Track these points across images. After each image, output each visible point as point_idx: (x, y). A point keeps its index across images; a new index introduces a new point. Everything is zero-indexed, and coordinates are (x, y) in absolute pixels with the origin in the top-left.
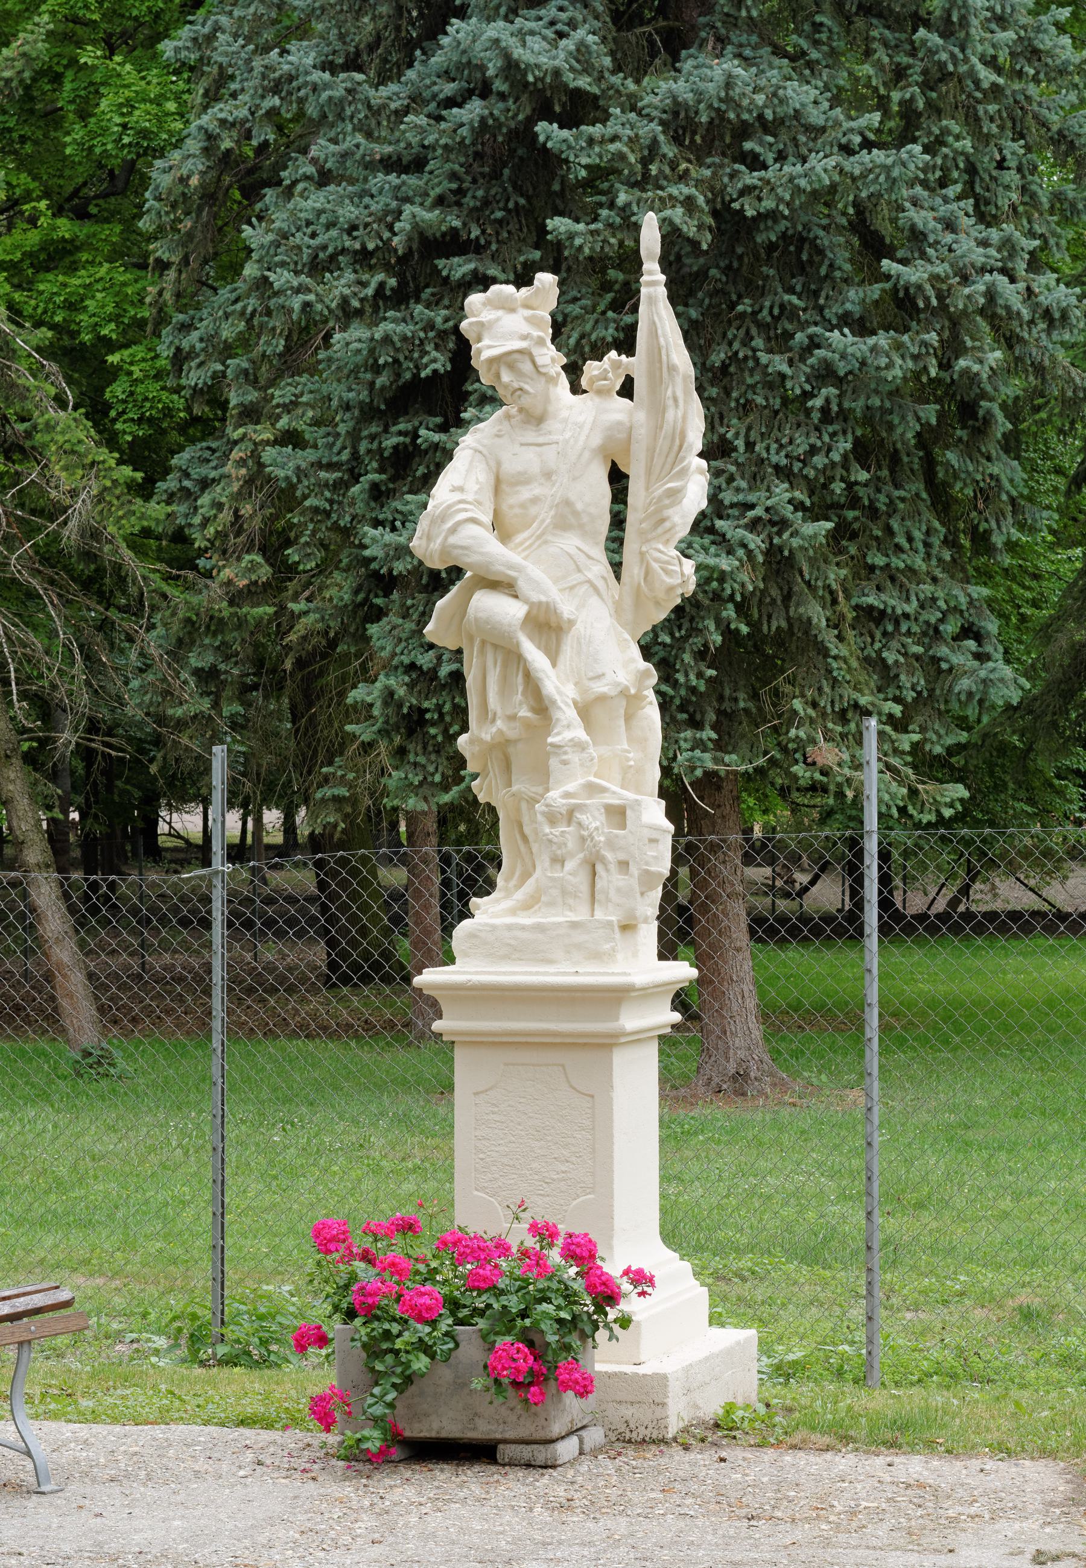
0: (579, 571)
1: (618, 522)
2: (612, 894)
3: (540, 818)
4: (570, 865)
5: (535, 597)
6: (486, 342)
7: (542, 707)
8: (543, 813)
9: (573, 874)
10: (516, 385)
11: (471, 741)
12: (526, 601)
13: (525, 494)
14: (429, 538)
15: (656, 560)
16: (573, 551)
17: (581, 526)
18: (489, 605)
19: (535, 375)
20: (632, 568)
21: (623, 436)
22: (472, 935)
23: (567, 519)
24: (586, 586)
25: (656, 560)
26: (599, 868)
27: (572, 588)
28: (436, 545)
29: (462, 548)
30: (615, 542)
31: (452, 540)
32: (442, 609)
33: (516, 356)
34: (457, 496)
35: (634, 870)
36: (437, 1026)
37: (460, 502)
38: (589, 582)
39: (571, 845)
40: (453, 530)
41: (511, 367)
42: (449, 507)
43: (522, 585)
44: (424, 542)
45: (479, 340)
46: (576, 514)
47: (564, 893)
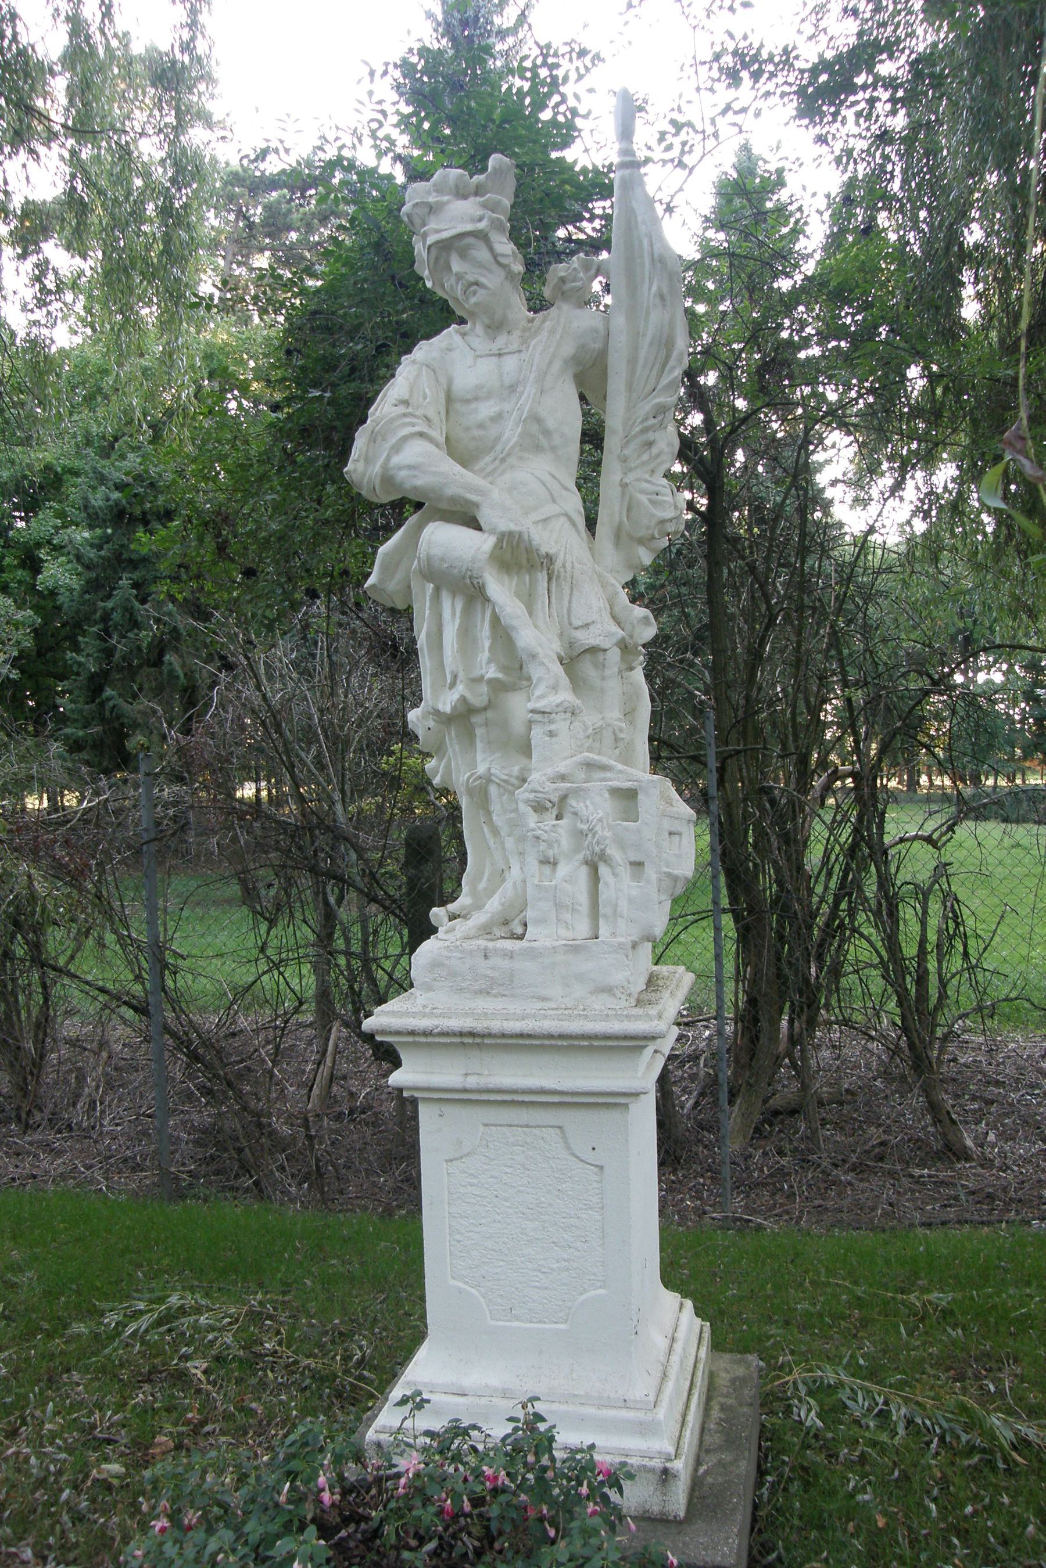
0: (554, 501)
1: (593, 436)
2: (624, 906)
3: (523, 808)
4: (563, 870)
5: (505, 525)
6: (432, 225)
7: (516, 669)
8: (527, 802)
9: (569, 880)
10: (471, 278)
11: (426, 715)
12: (492, 532)
13: (486, 410)
14: (368, 460)
15: (643, 492)
16: (546, 478)
17: (553, 449)
18: (442, 539)
19: (494, 267)
20: (607, 515)
21: (598, 346)
22: (435, 965)
23: (536, 438)
24: (563, 519)
25: (643, 492)
26: (603, 870)
27: (545, 520)
28: (377, 468)
29: (410, 467)
30: (588, 478)
31: (396, 460)
32: (386, 554)
33: (471, 240)
34: (402, 409)
35: (651, 872)
36: (396, 1078)
37: (405, 415)
38: (566, 515)
39: (566, 843)
40: (397, 448)
41: (463, 255)
42: (392, 420)
43: (485, 516)
44: (360, 466)
45: (424, 225)
46: (547, 433)
47: (559, 906)
